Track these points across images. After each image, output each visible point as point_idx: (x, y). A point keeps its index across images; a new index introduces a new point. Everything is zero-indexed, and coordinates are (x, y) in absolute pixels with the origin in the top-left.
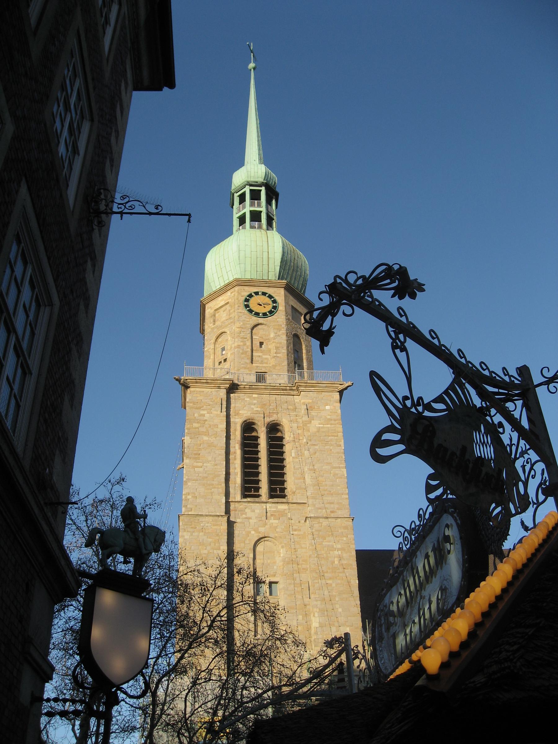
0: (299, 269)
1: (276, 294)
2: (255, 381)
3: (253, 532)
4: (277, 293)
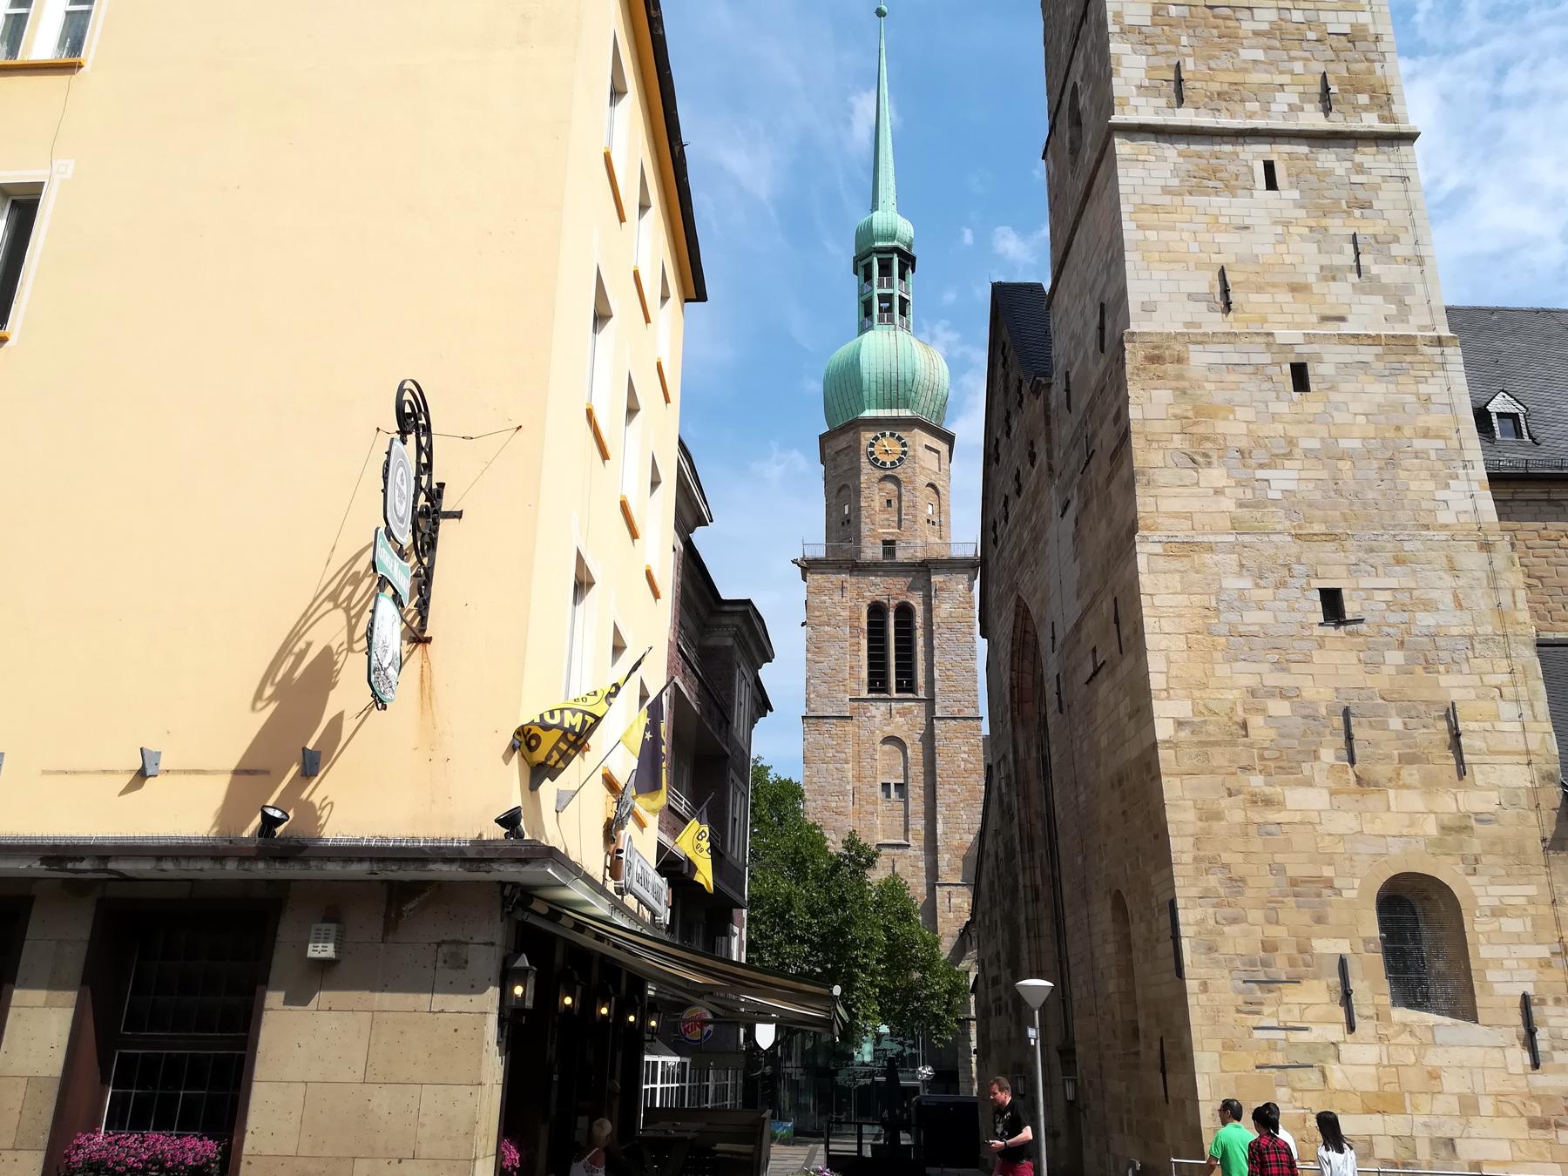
0: (936, 387)
2: (881, 556)
3: (877, 732)
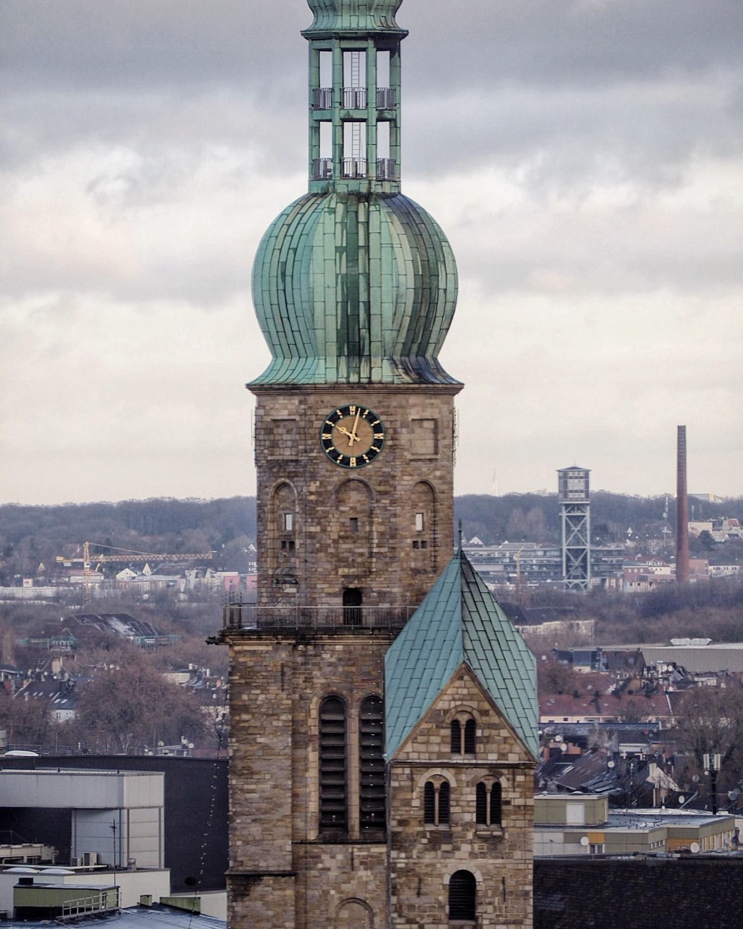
1: (382, 410)
3: (333, 892)
4: (383, 406)
